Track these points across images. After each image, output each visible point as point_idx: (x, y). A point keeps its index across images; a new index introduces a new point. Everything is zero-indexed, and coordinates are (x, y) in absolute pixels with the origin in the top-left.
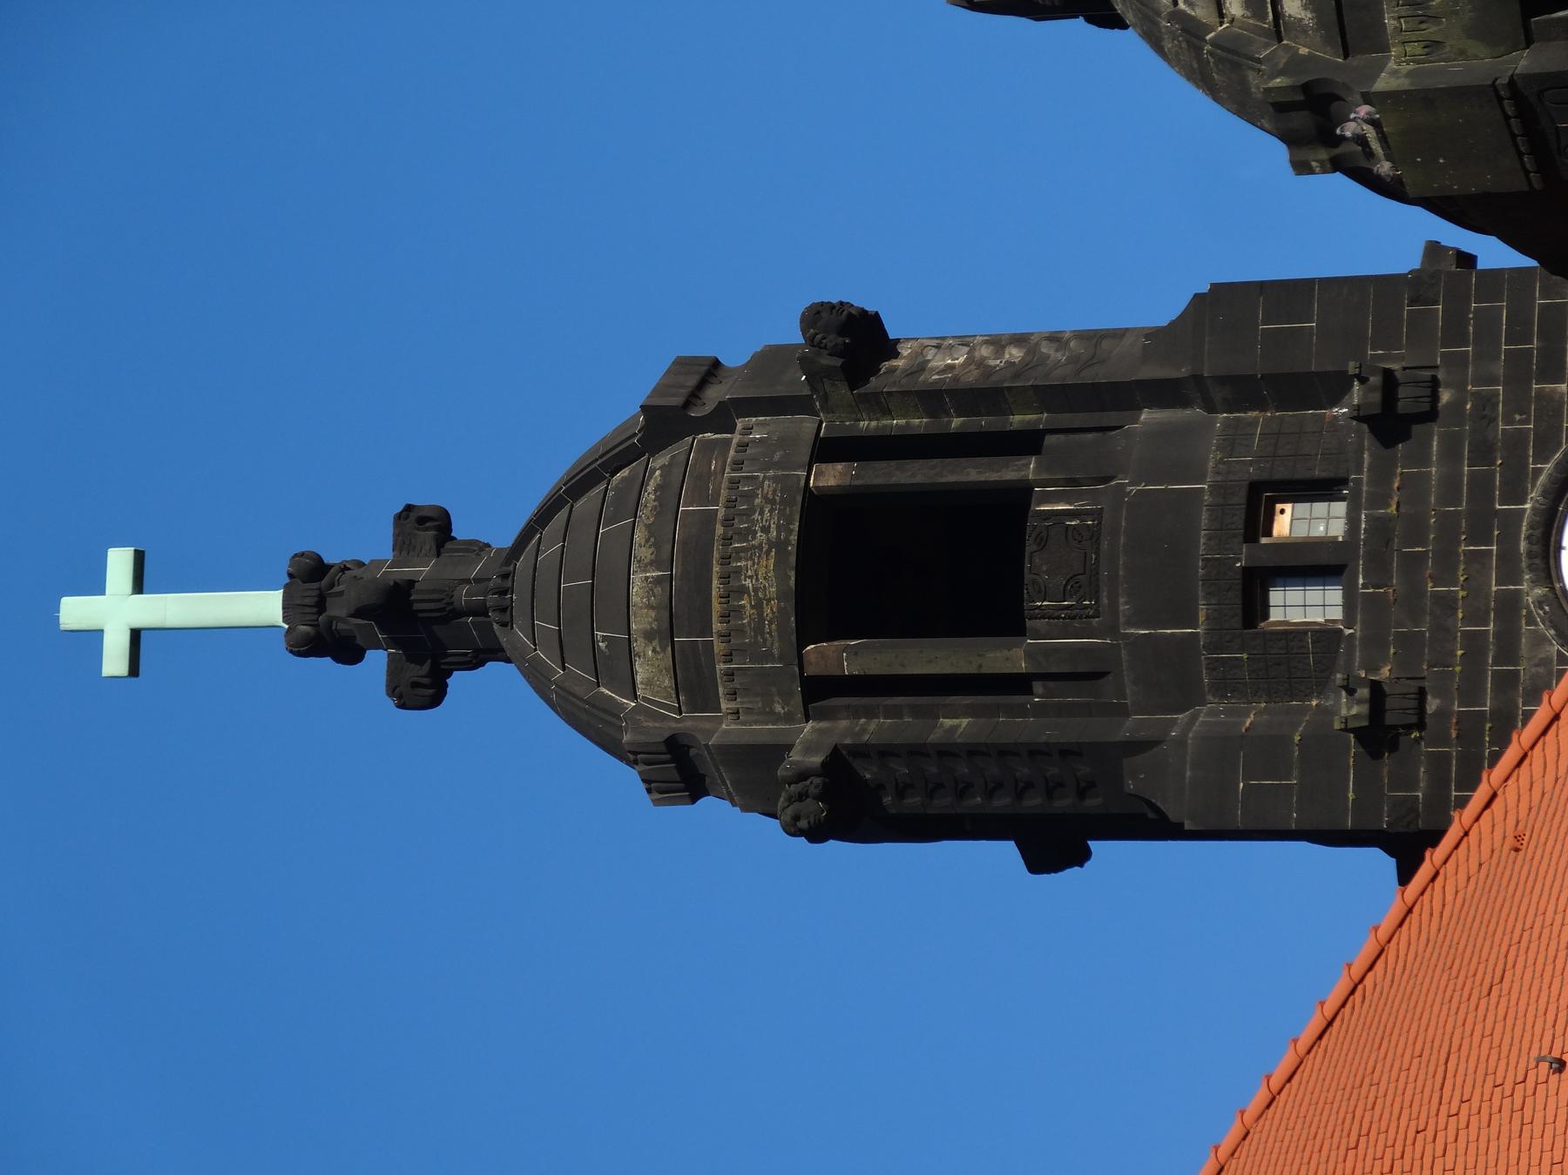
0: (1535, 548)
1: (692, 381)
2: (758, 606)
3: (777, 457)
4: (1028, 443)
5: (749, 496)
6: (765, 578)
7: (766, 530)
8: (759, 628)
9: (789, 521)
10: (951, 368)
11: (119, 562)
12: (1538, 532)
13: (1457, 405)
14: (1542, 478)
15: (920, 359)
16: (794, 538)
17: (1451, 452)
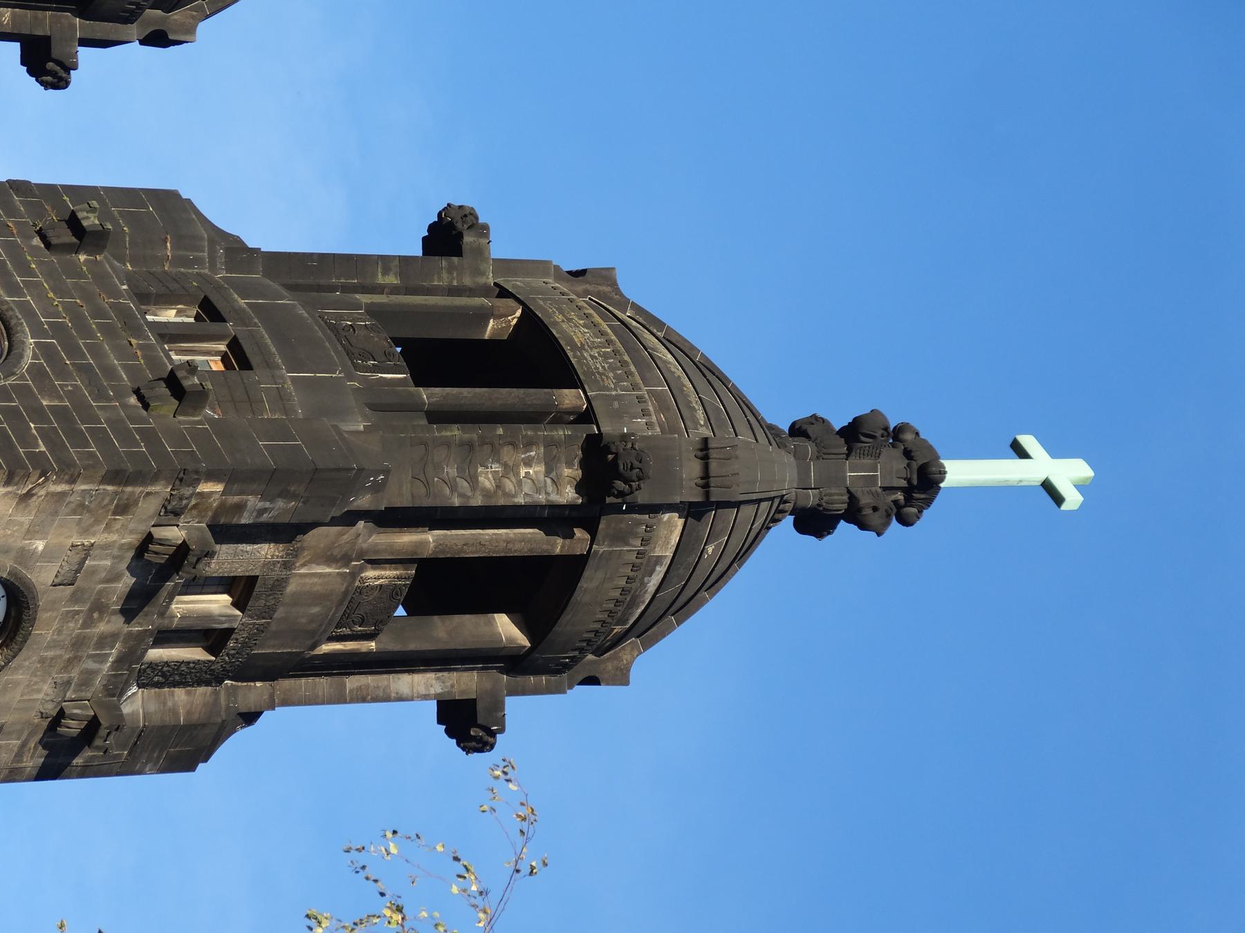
0: (10, 313)
1: (713, 465)
2: (570, 320)
3: (616, 404)
4: (438, 416)
5: (619, 379)
6: (576, 332)
7: (593, 357)
8: (561, 312)
9: (578, 362)
10: (528, 463)
11: (1073, 500)
12: (13, 322)
13: (120, 395)
14: (29, 353)
15: (553, 475)
16: (570, 354)
17: (110, 372)
